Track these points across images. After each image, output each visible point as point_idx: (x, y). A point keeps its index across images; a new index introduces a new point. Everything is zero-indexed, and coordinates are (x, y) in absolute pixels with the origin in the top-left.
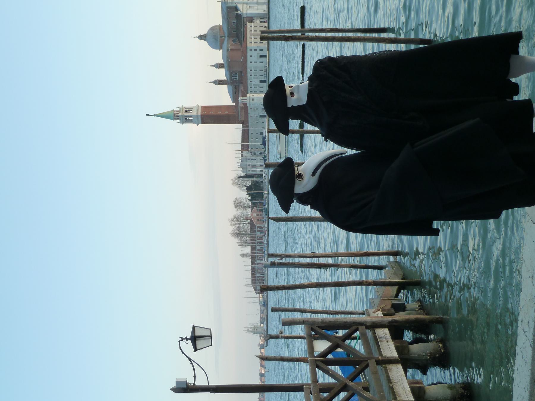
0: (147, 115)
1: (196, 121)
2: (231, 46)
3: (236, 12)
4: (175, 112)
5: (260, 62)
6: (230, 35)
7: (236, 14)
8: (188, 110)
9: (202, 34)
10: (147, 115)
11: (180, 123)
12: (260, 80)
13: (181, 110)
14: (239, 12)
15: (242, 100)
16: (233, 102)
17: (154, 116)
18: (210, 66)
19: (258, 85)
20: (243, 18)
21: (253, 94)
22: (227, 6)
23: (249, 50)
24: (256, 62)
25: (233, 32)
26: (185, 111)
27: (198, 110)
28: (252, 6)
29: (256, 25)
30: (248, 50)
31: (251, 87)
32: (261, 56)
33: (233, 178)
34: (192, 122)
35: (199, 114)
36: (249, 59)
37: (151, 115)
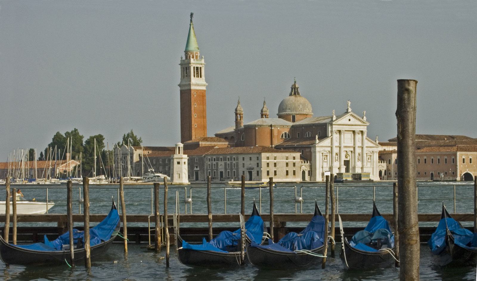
0: (192, 15)
1: (184, 83)
2: (278, 130)
3: (317, 137)
4: (196, 53)
5: (244, 172)
7: (315, 137)
8: (198, 71)
10: (192, 15)
11: (181, 60)
13: (199, 62)
14: (317, 141)
15: (179, 148)
16: (217, 135)
18: (264, 102)
19: (217, 170)
20: (310, 147)
21: (187, 163)
22: (327, 124)
23: (258, 156)
24: (244, 167)
25: (298, 133)
26: (197, 67)
27: (198, 85)
28: (327, 159)
30: (258, 156)
31: (215, 159)
32: (250, 173)
34: (183, 78)
35: (193, 88)
36: (247, 157)
37: (191, 21)
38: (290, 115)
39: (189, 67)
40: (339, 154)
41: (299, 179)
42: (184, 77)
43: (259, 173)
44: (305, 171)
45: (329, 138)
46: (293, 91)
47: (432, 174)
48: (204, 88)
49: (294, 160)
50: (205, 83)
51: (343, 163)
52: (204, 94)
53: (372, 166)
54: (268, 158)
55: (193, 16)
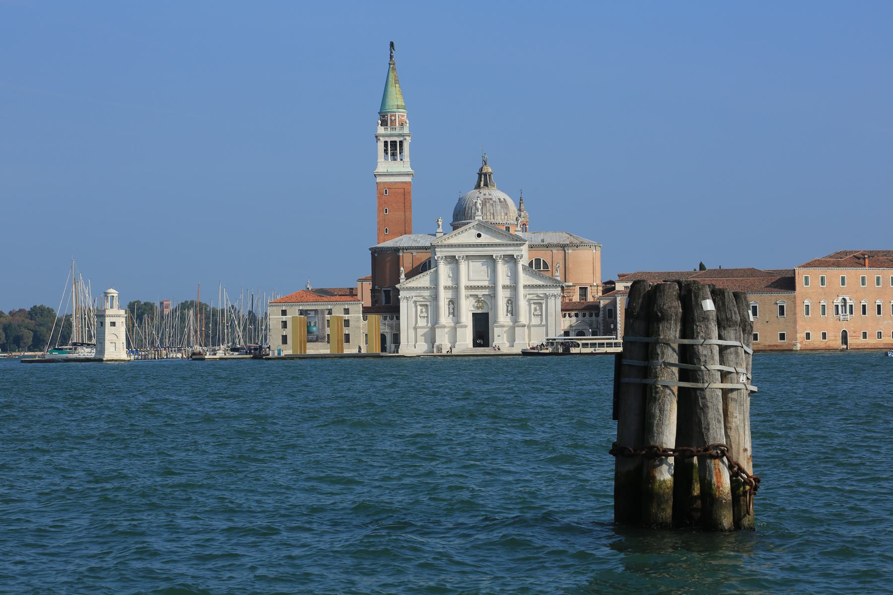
4: (391, 116)
10: (392, 44)
13: (397, 132)
26: (391, 142)
27: (392, 175)
29: (351, 323)
37: (391, 57)
40: (454, 304)
44: (385, 334)
45: (428, 272)
46: (483, 179)
48: (408, 179)
49: (347, 316)
50: (410, 170)
51: (467, 319)
52: (406, 189)
53: (544, 322)
54: (284, 313)
55: (395, 47)
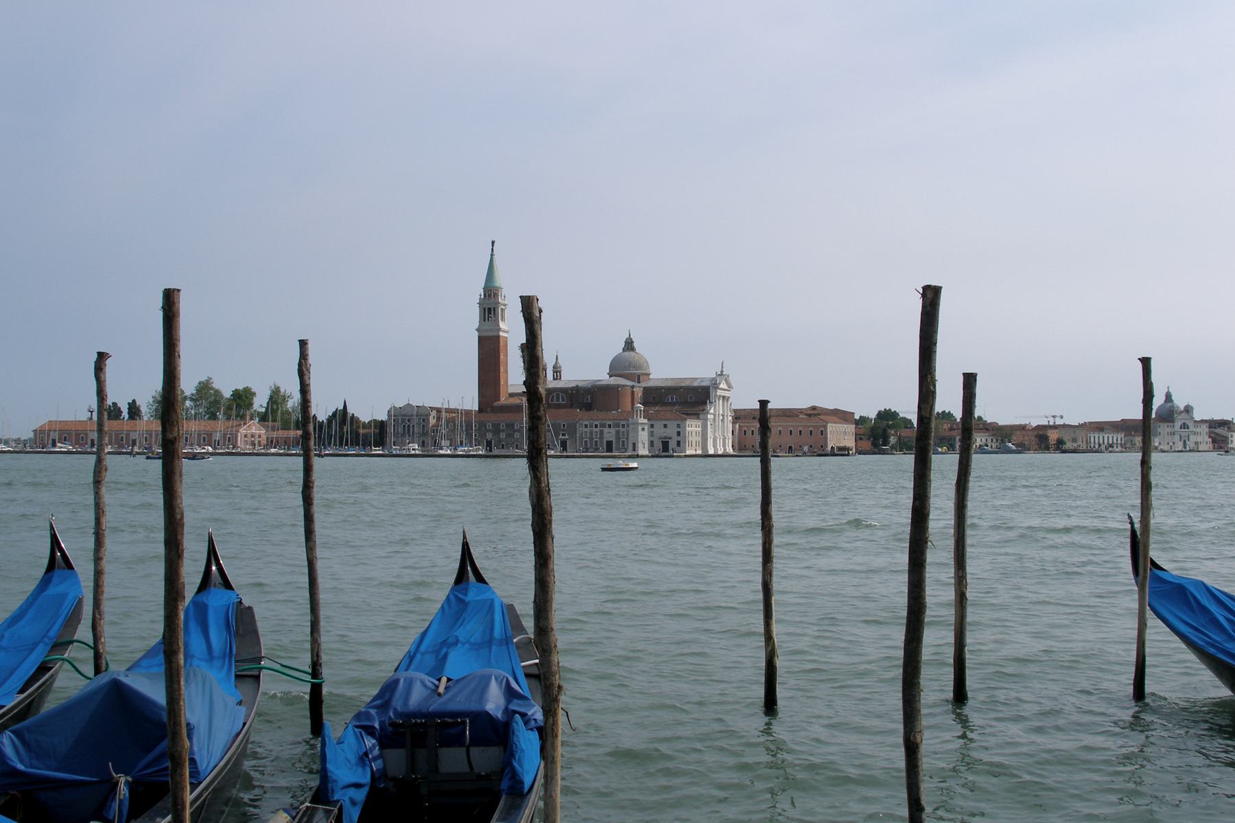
0: (493, 243)
6: (647, 391)
9: (635, 345)
11: (480, 298)
12: (612, 441)
17: (490, 253)
18: (557, 356)
19: (601, 438)
20: (699, 414)
22: (711, 388)
23: (679, 422)
30: (679, 422)
33: (282, 390)
35: (501, 334)
36: (659, 425)
37: (492, 249)
38: (635, 374)
39: (494, 309)
41: (699, 452)
42: (485, 320)
43: (681, 444)
47: (790, 447)
